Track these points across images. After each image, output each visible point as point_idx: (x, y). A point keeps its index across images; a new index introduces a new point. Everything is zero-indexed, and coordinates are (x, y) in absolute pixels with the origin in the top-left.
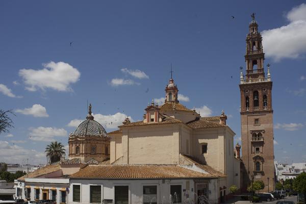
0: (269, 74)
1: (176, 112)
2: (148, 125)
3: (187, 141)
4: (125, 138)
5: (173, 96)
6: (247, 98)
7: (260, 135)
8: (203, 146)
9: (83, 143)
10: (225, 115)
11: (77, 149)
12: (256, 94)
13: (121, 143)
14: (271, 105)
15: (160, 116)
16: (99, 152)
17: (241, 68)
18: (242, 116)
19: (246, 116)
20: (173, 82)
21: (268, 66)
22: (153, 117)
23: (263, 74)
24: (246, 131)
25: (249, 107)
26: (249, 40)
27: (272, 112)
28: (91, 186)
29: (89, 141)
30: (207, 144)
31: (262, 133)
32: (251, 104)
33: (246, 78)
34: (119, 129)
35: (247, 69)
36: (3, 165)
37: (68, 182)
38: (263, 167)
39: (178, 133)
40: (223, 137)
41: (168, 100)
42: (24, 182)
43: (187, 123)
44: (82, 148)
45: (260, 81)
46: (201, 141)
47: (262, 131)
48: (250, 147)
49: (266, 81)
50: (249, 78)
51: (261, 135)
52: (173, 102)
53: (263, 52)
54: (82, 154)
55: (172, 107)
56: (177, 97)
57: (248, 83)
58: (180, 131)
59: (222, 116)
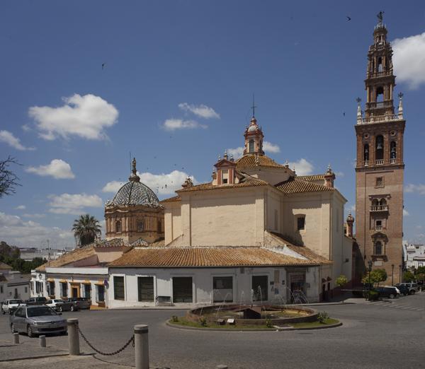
0: (400, 109)
1: (261, 168)
2: (219, 188)
4: (185, 208)
5: (255, 144)
6: (366, 147)
7: (383, 202)
8: (298, 219)
9: (125, 217)
10: (332, 172)
11: (118, 224)
12: (380, 139)
13: (180, 215)
14: (401, 156)
17: (359, 100)
18: (358, 173)
19: (363, 173)
20: (255, 124)
21: (401, 95)
22: (226, 176)
23: (392, 109)
24: (363, 196)
26: (373, 54)
27: (402, 167)
28: (138, 278)
30: (305, 215)
31: (386, 199)
32: (372, 155)
33: (366, 115)
34: (177, 195)
35: (368, 102)
36: (14, 249)
37: (107, 273)
38: (386, 248)
39: (263, 200)
40: (328, 205)
42: (45, 272)
43: (276, 186)
44: (125, 223)
45: (386, 120)
46: (296, 212)
47: (386, 195)
48: (368, 220)
49: (396, 120)
50: (370, 115)
51: (386, 202)
52: (256, 153)
53: (394, 75)
54: (125, 232)
55: (254, 161)
56: (261, 146)
57: (369, 123)
58: (265, 197)
59: (329, 174)
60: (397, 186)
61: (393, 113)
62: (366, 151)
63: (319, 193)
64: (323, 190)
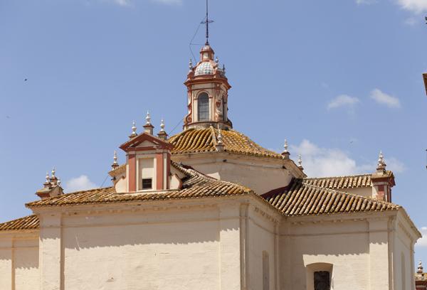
1: (227, 156)
2: (134, 199)
3: (265, 256)
4: (49, 247)
5: (211, 103)
13: (36, 265)
15: (173, 170)
20: (211, 58)
22: (150, 172)
30: (331, 266)
39: (238, 232)
40: (385, 246)
41: (195, 119)
43: (267, 196)
46: (309, 260)
52: (213, 123)
56: (224, 110)
58: (243, 223)
59: (380, 174)
63: (362, 216)
64: (374, 209)
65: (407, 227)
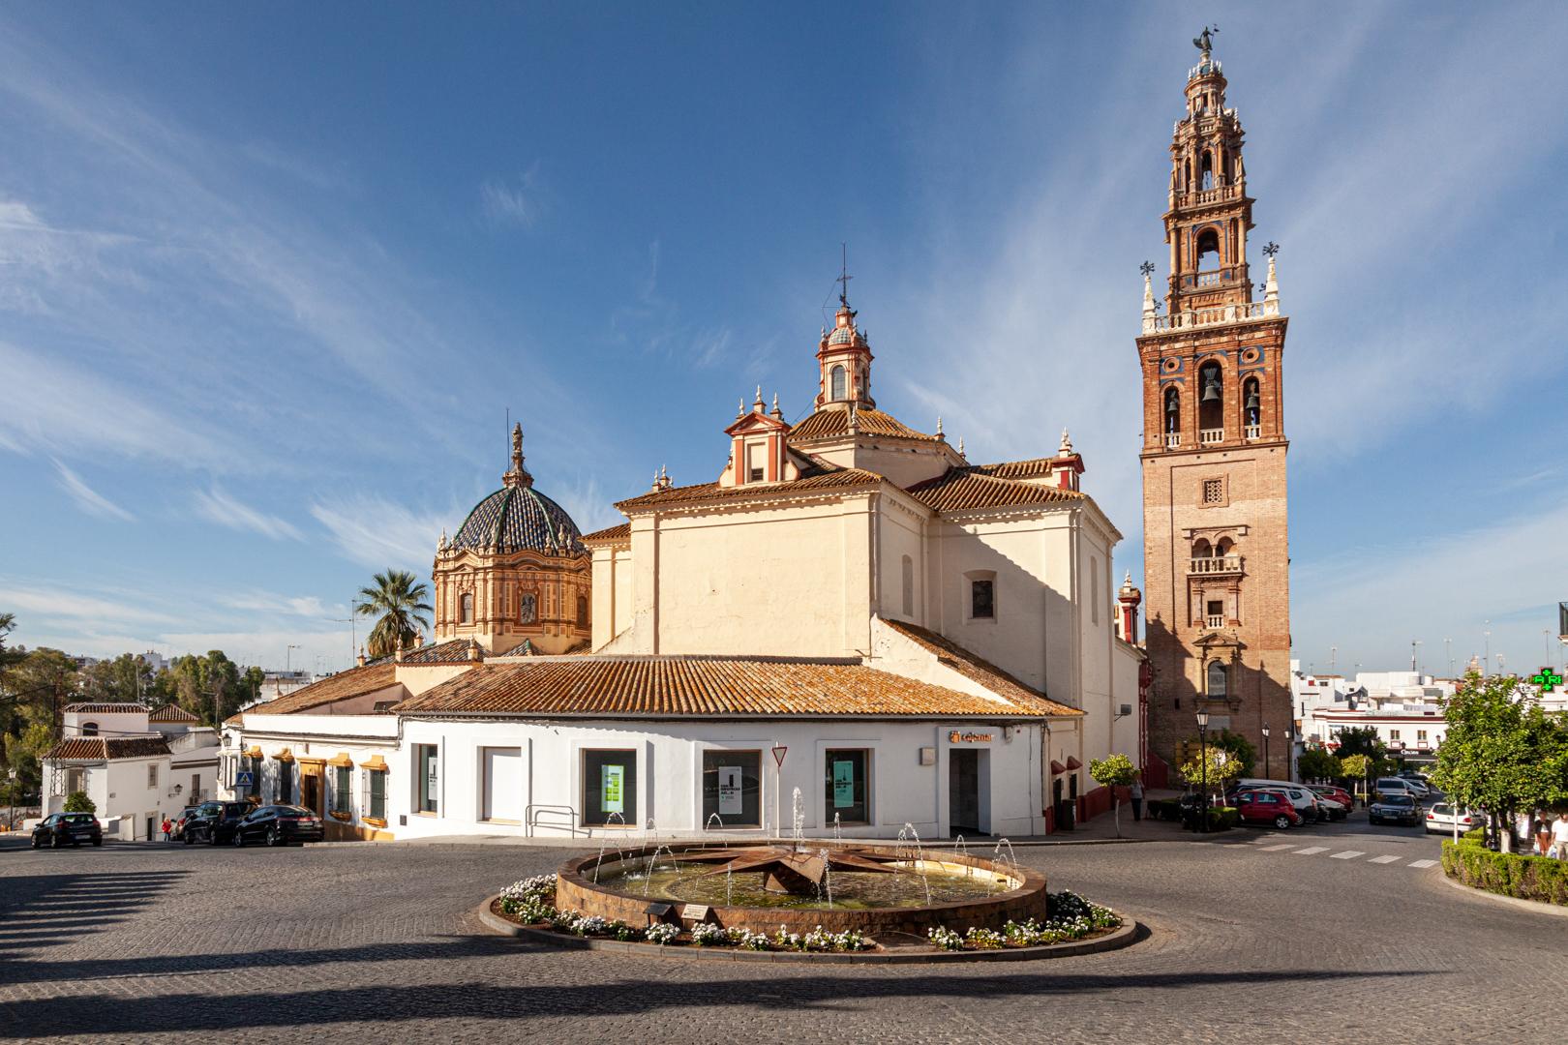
14: (1278, 418)
16: (552, 616)
17: (1147, 268)
21: (1271, 250)
25: (1177, 429)
29: (509, 573)
32: (1189, 414)
45: (1230, 319)
53: (1248, 195)
60: (1269, 501)
61: (1249, 300)
62: (1172, 408)
65: (1105, 530)
